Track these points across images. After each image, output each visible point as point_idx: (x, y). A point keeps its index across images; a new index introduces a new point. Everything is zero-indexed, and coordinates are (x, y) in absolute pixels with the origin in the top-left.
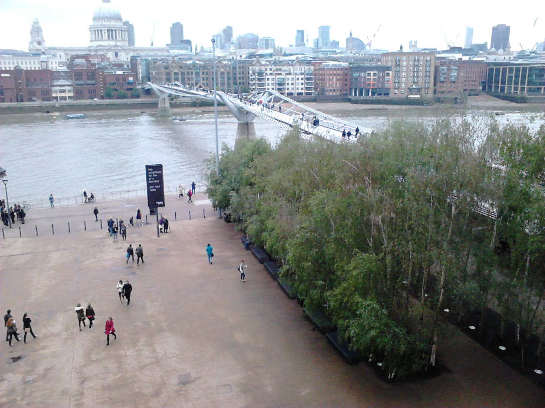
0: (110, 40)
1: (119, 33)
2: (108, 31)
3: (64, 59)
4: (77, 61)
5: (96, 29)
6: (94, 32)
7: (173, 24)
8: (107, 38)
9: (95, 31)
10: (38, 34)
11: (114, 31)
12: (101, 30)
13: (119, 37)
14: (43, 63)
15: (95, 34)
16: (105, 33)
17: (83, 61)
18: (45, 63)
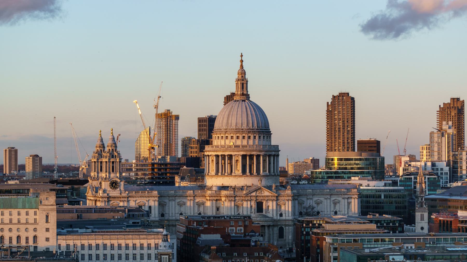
0: (247, 176)
1: (264, 161)
2: (244, 157)
3: (157, 215)
4: (204, 237)
5: (220, 153)
6: (214, 158)
7: (334, 97)
8: (240, 172)
9: (217, 156)
10: (113, 167)
11: (255, 158)
12: (230, 157)
13: (264, 171)
14: (163, 256)
15: (217, 163)
16: (237, 161)
17: (217, 237)
18: (167, 256)
